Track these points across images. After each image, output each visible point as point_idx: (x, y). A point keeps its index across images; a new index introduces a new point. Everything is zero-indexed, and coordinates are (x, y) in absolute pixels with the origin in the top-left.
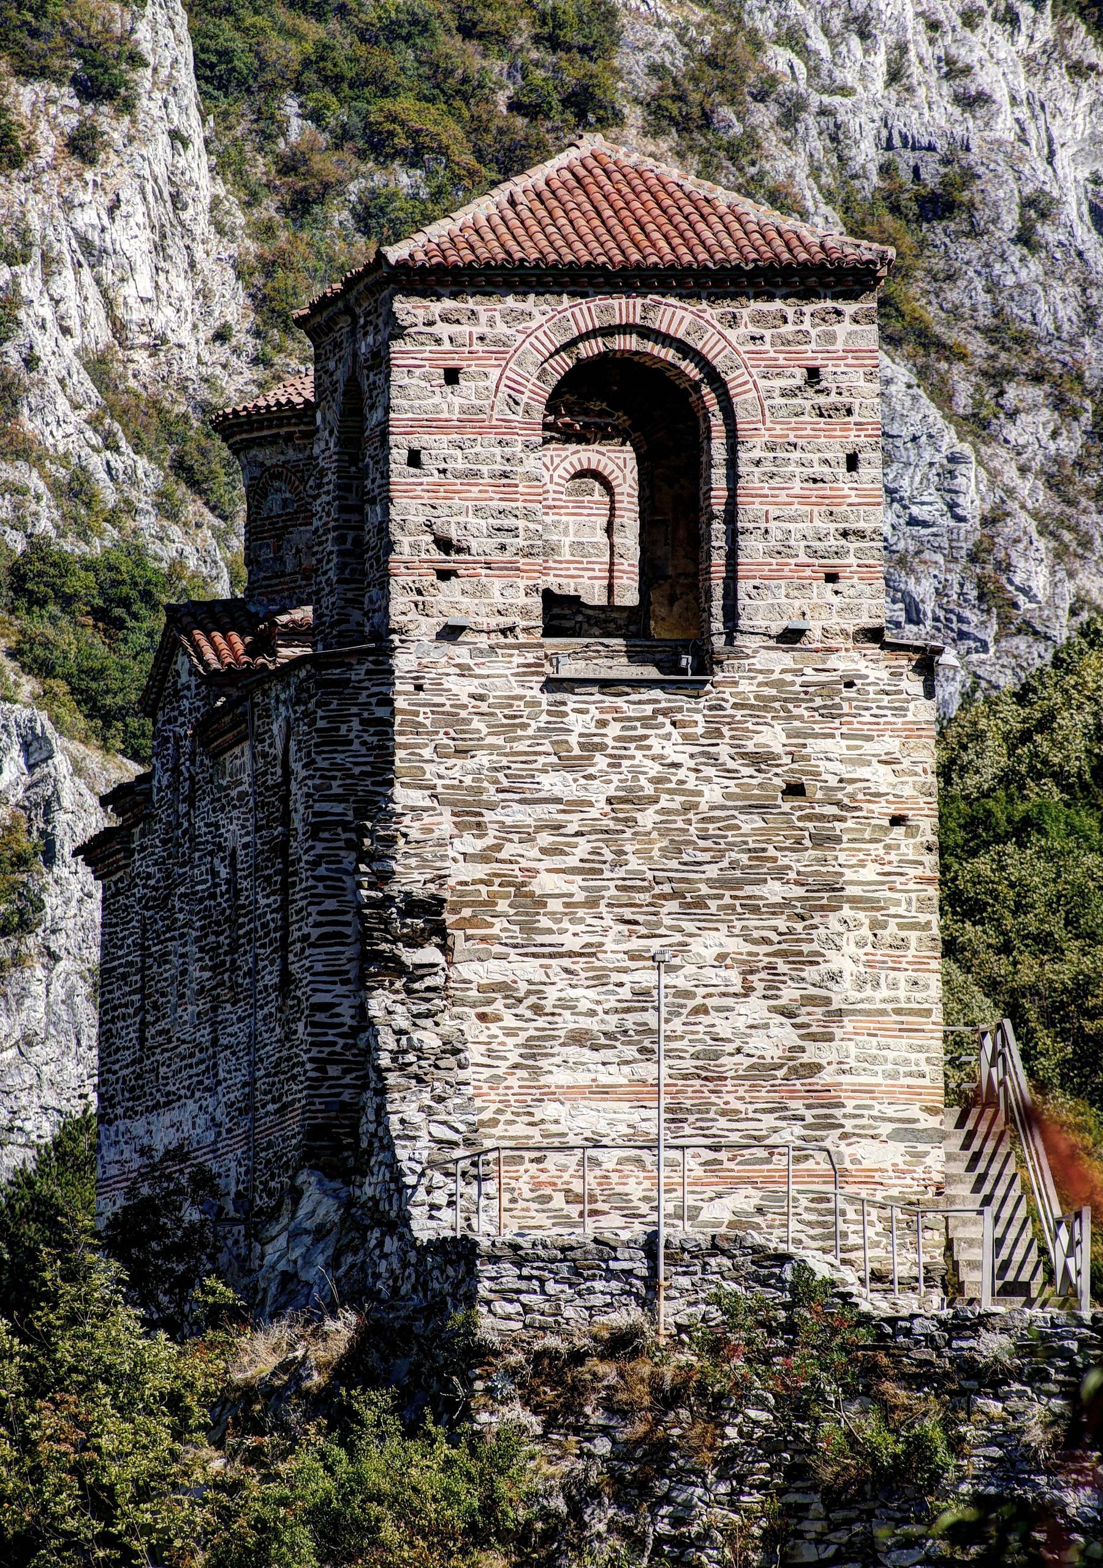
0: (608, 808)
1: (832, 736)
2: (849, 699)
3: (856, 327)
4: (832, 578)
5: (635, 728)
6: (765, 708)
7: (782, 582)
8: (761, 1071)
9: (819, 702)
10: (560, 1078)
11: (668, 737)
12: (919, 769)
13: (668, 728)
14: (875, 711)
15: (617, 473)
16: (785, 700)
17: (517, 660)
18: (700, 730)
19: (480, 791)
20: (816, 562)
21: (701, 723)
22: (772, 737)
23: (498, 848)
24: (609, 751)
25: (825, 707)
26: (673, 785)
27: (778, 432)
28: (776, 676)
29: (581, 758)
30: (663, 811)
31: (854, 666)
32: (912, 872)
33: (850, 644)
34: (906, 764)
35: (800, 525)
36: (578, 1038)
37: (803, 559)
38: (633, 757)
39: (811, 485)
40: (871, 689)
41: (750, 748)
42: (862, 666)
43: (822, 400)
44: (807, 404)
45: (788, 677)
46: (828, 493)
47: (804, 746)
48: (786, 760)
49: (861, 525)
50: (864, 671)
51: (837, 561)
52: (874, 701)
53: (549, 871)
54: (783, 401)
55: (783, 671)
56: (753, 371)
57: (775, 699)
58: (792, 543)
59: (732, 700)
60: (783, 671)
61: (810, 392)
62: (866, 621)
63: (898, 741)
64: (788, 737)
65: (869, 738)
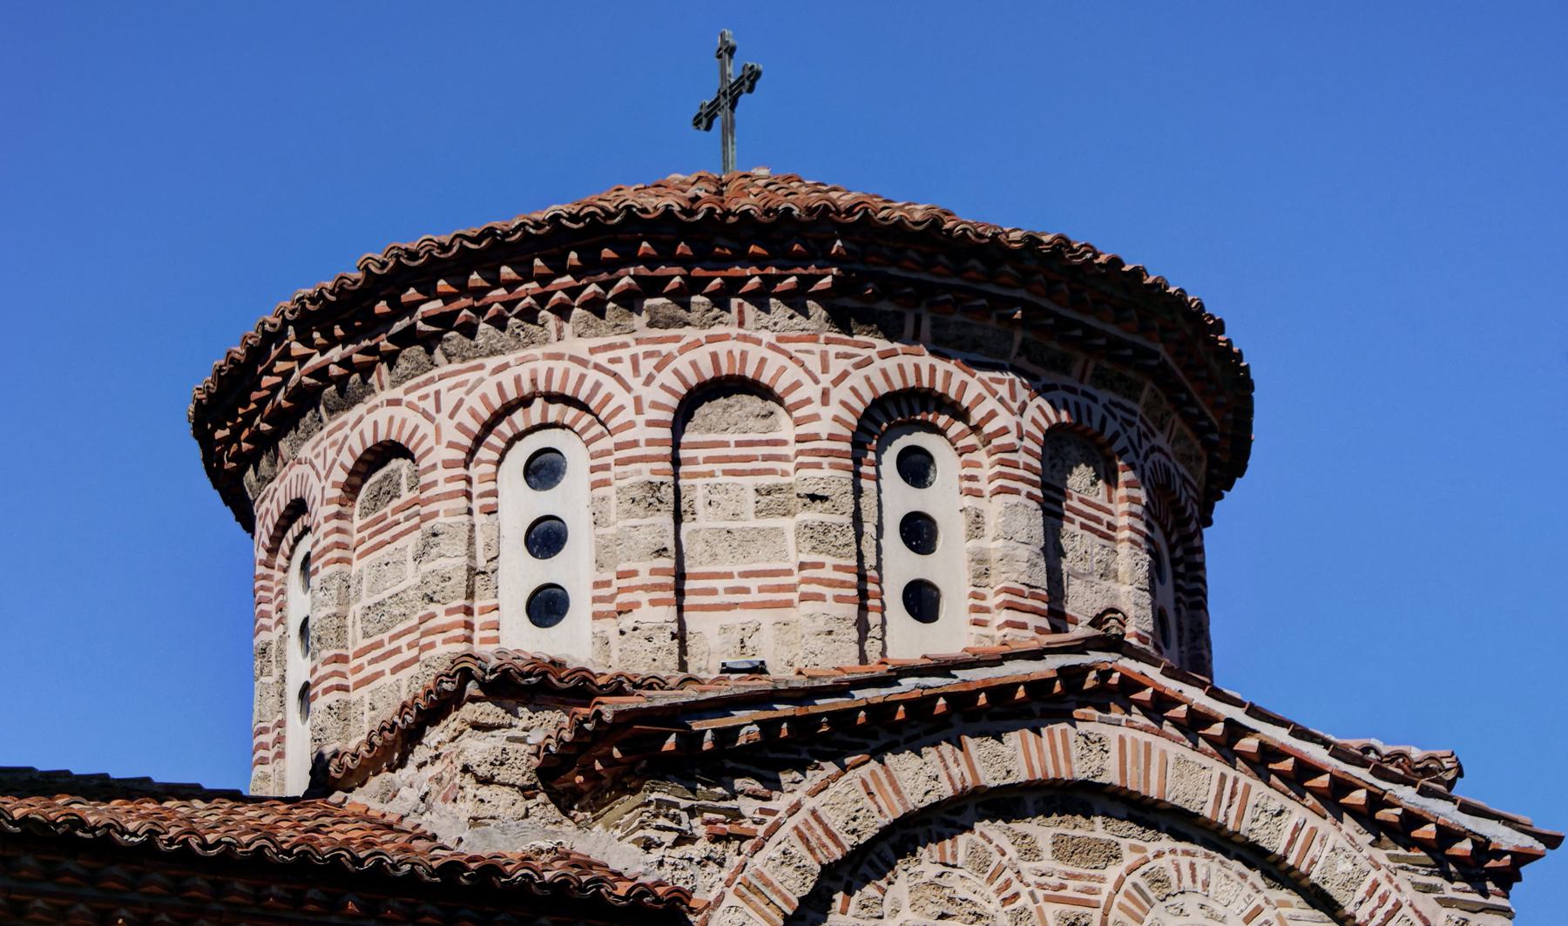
15: (426, 428)
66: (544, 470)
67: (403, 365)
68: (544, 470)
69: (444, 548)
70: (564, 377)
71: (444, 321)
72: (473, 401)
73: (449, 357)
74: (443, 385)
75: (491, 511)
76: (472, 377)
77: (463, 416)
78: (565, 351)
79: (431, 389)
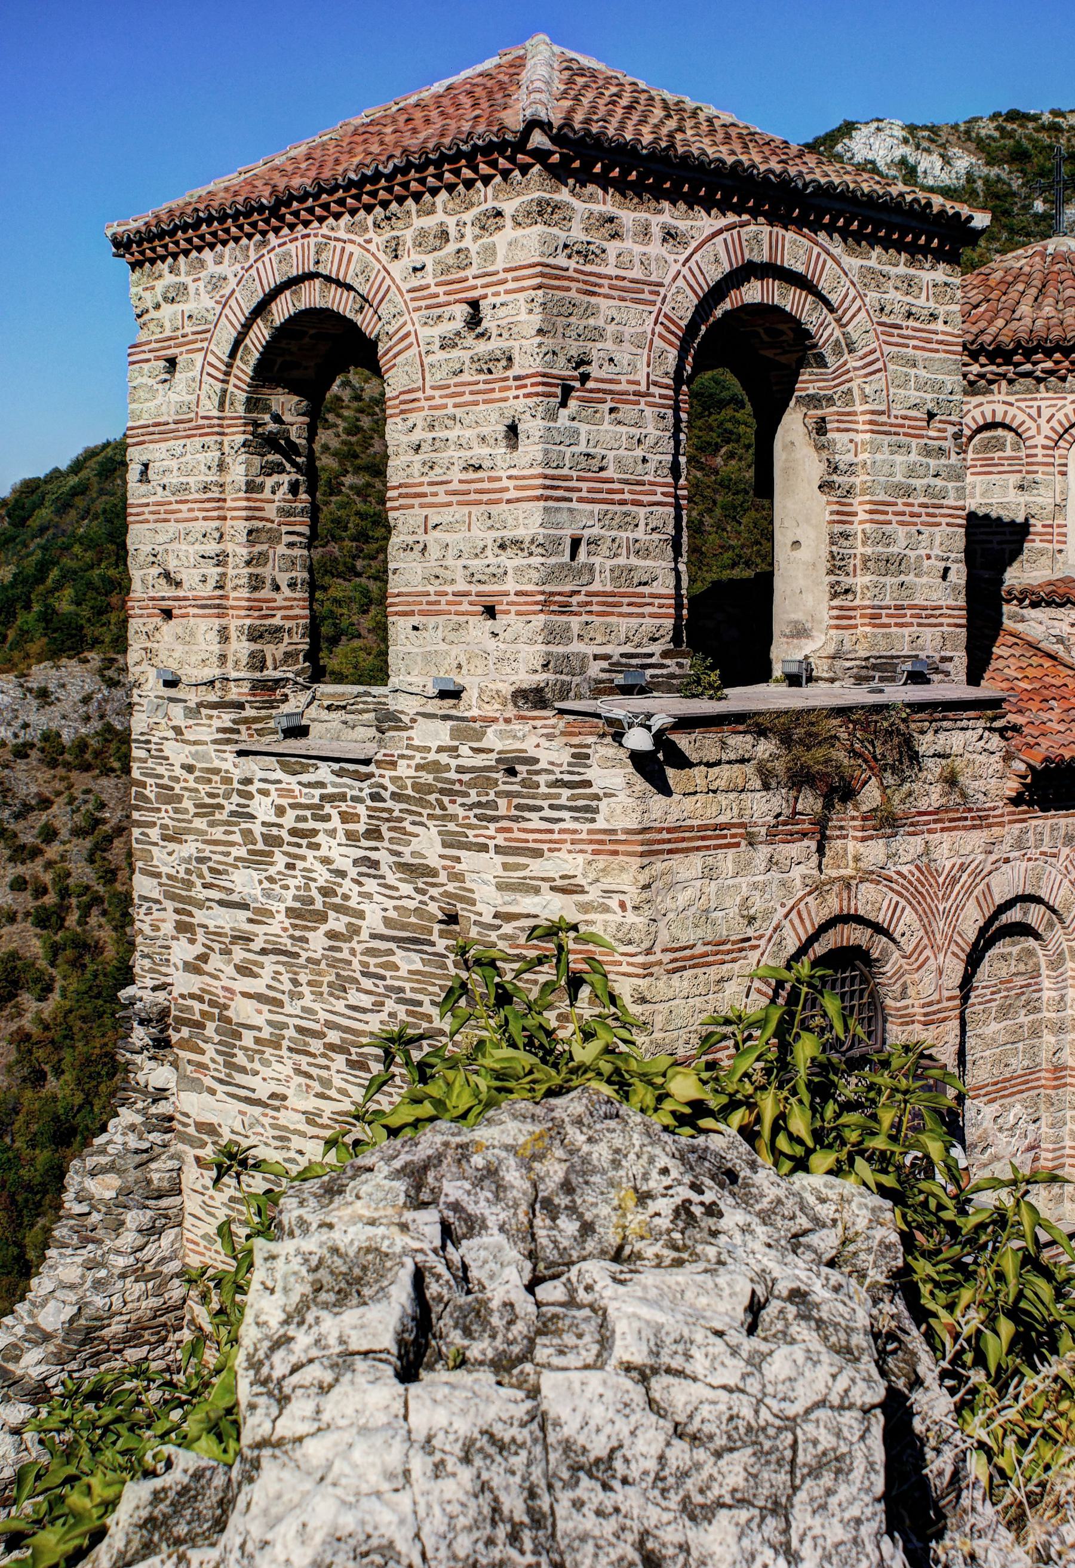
0: (287, 923)
1: (484, 848)
2: (509, 795)
3: (520, 232)
4: (490, 612)
5: (304, 819)
6: (422, 802)
7: (440, 619)
9: (474, 798)
11: (332, 833)
12: (614, 903)
13: (336, 822)
14: (548, 813)
15: (1029, 423)
16: (442, 791)
17: (217, 723)
18: (361, 827)
19: (189, 885)
20: (475, 588)
21: (364, 819)
22: (427, 844)
23: (204, 958)
24: (285, 848)
25: (479, 805)
26: (337, 900)
27: (438, 401)
28: (432, 756)
29: (261, 853)
30: (332, 935)
31: (518, 745)
33: (511, 712)
34: (593, 894)
35: (458, 536)
37: (462, 586)
38: (303, 858)
39: (471, 475)
40: (542, 779)
41: (407, 859)
42: (529, 746)
43: (482, 347)
44: (466, 355)
45: (444, 758)
46: (486, 485)
47: (458, 860)
48: (443, 878)
49: (520, 533)
50: (532, 752)
51: (496, 588)
52: (547, 796)
53: (245, 995)
54: (441, 355)
55: (440, 750)
56: (415, 316)
57: (429, 789)
58: (450, 562)
59: (392, 788)
60: (440, 750)
61: (470, 340)
62: (528, 681)
63: (580, 858)
64: (445, 845)
65: (538, 854)
67: (1017, 387)
69: (1042, 491)
71: (1051, 372)
72: (1060, 416)
73: (1047, 390)
74: (1044, 404)
75: (1064, 474)
76: (1060, 403)
77: (1054, 423)
79: (1036, 404)
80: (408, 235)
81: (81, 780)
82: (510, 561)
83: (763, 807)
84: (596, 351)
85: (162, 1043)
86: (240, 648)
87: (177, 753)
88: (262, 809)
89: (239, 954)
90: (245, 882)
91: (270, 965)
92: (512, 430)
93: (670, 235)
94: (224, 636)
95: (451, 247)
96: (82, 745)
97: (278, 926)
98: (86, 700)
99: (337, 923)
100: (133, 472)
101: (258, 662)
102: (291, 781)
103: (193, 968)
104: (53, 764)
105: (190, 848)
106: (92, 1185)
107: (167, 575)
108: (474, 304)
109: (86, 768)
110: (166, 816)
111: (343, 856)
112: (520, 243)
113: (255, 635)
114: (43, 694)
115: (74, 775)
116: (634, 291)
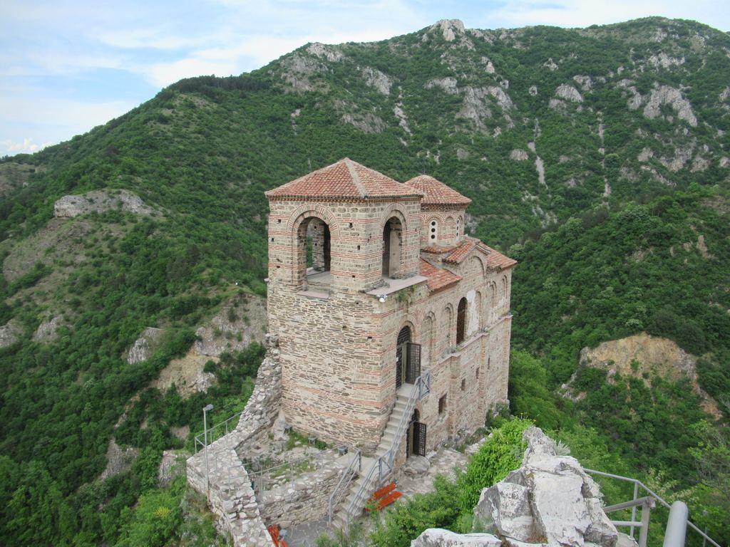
4: (354, 277)
8: (337, 392)
10: (299, 383)
22: (340, 314)
32: (373, 351)
36: (302, 376)
43: (353, 231)
66: (433, 224)
68: (433, 224)
70: (437, 216)
78: (438, 213)
80: (337, 208)
81: (104, 225)
82: (359, 269)
83: (396, 306)
84: (372, 232)
85: (277, 346)
86: (296, 275)
87: (281, 293)
88: (302, 305)
89: (296, 330)
90: (298, 318)
91: (303, 333)
92: (359, 247)
93: (382, 209)
94: (292, 272)
95: (346, 213)
96: (105, 215)
97: (305, 326)
98: (104, 202)
99: (321, 327)
100: (270, 239)
101: (299, 277)
102: (310, 301)
103: (285, 332)
104: (96, 220)
105: (284, 310)
106: (265, 373)
107: (278, 260)
108: (351, 224)
109: (106, 222)
110: (279, 304)
111: (321, 315)
112: (363, 215)
113: (299, 273)
114: (91, 201)
115: (102, 224)
116: (377, 220)
